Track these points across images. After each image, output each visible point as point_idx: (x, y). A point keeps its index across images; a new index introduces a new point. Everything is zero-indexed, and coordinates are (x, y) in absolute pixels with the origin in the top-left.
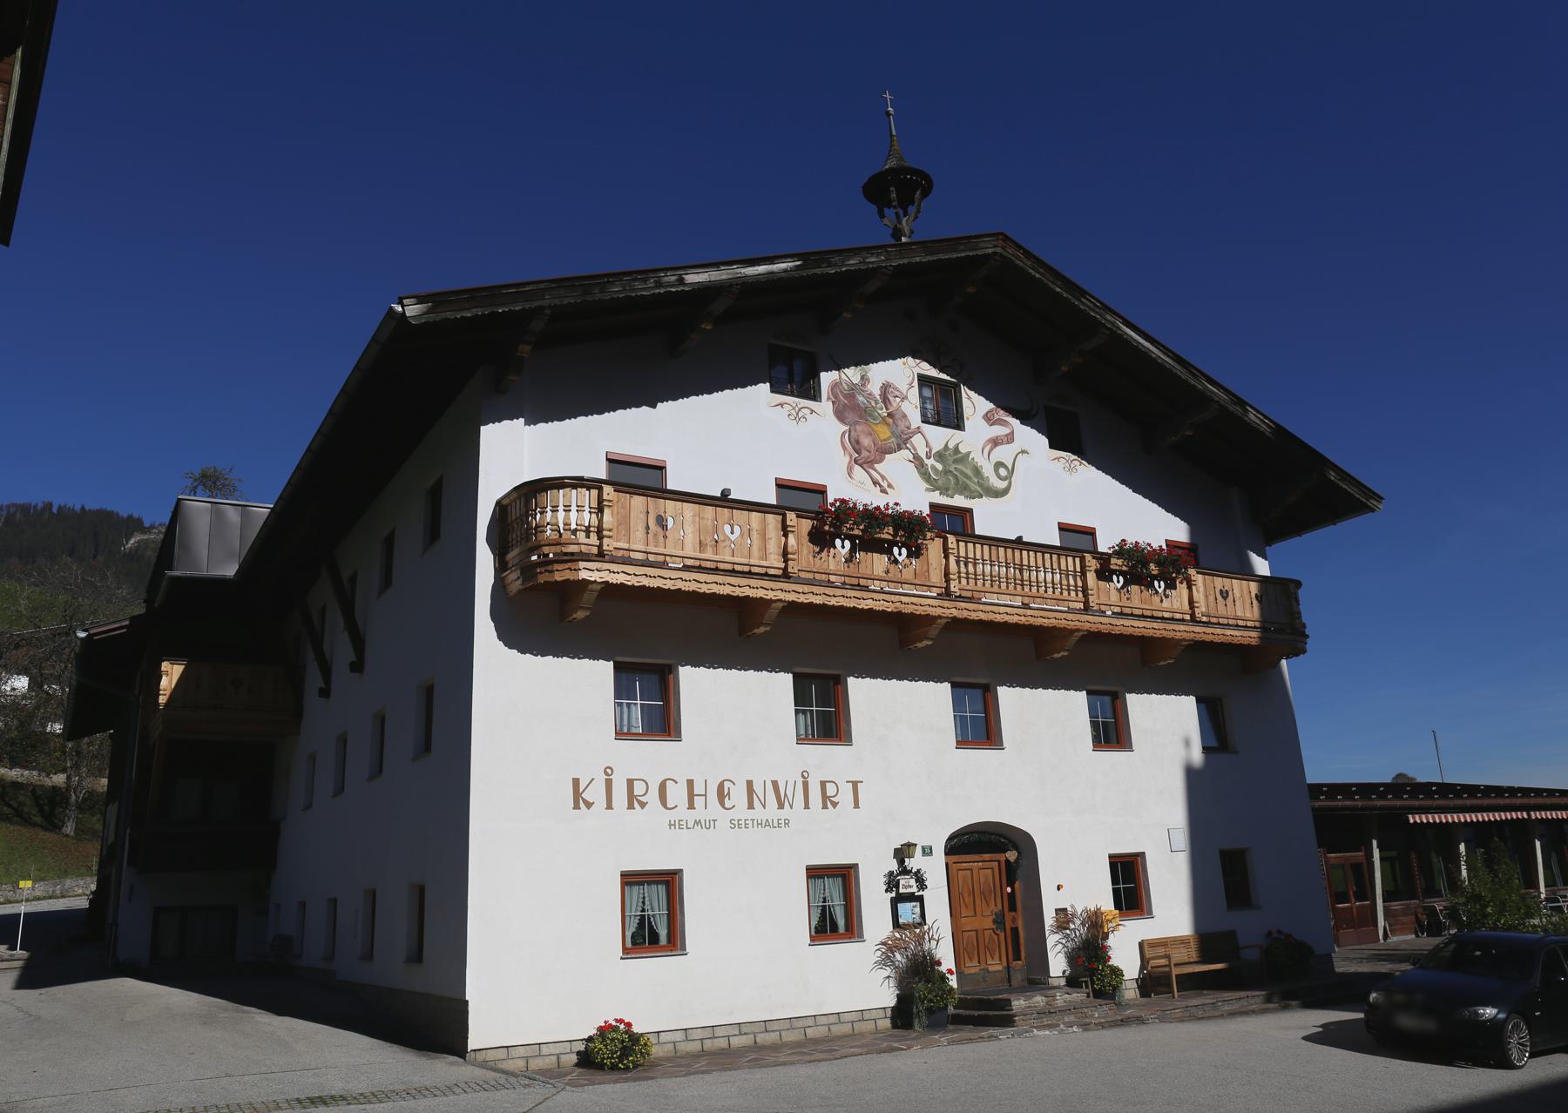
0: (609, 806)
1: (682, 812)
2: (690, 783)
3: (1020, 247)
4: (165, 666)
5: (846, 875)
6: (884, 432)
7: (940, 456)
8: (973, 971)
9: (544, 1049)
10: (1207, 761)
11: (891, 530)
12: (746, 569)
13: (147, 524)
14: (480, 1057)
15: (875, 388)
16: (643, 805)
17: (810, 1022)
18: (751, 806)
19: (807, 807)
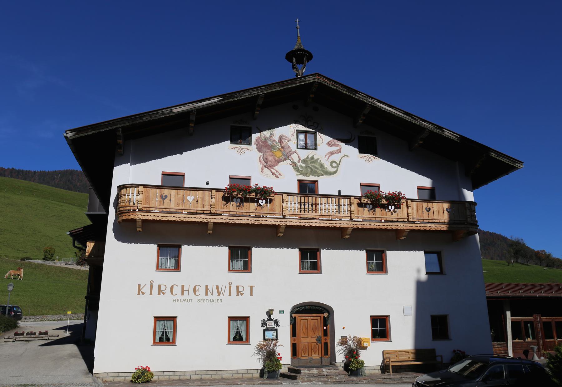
0: (151, 294)
1: (179, 296)
2: (183, 286)
3: (326, 78)
4: (88, 243)
5: (246, 320)
6: (279, 154)
7: (304, 161)
8: (305, 358)
9: (121, 375)
10: (429, 279)
11: (254, 194)
12: (195, 211)
13: (187, 183)
14: (97, 375)
15: (276, 138)
16: (164, 294)
17: (225, 372)
18: (207, 294)
19: (230, 295)
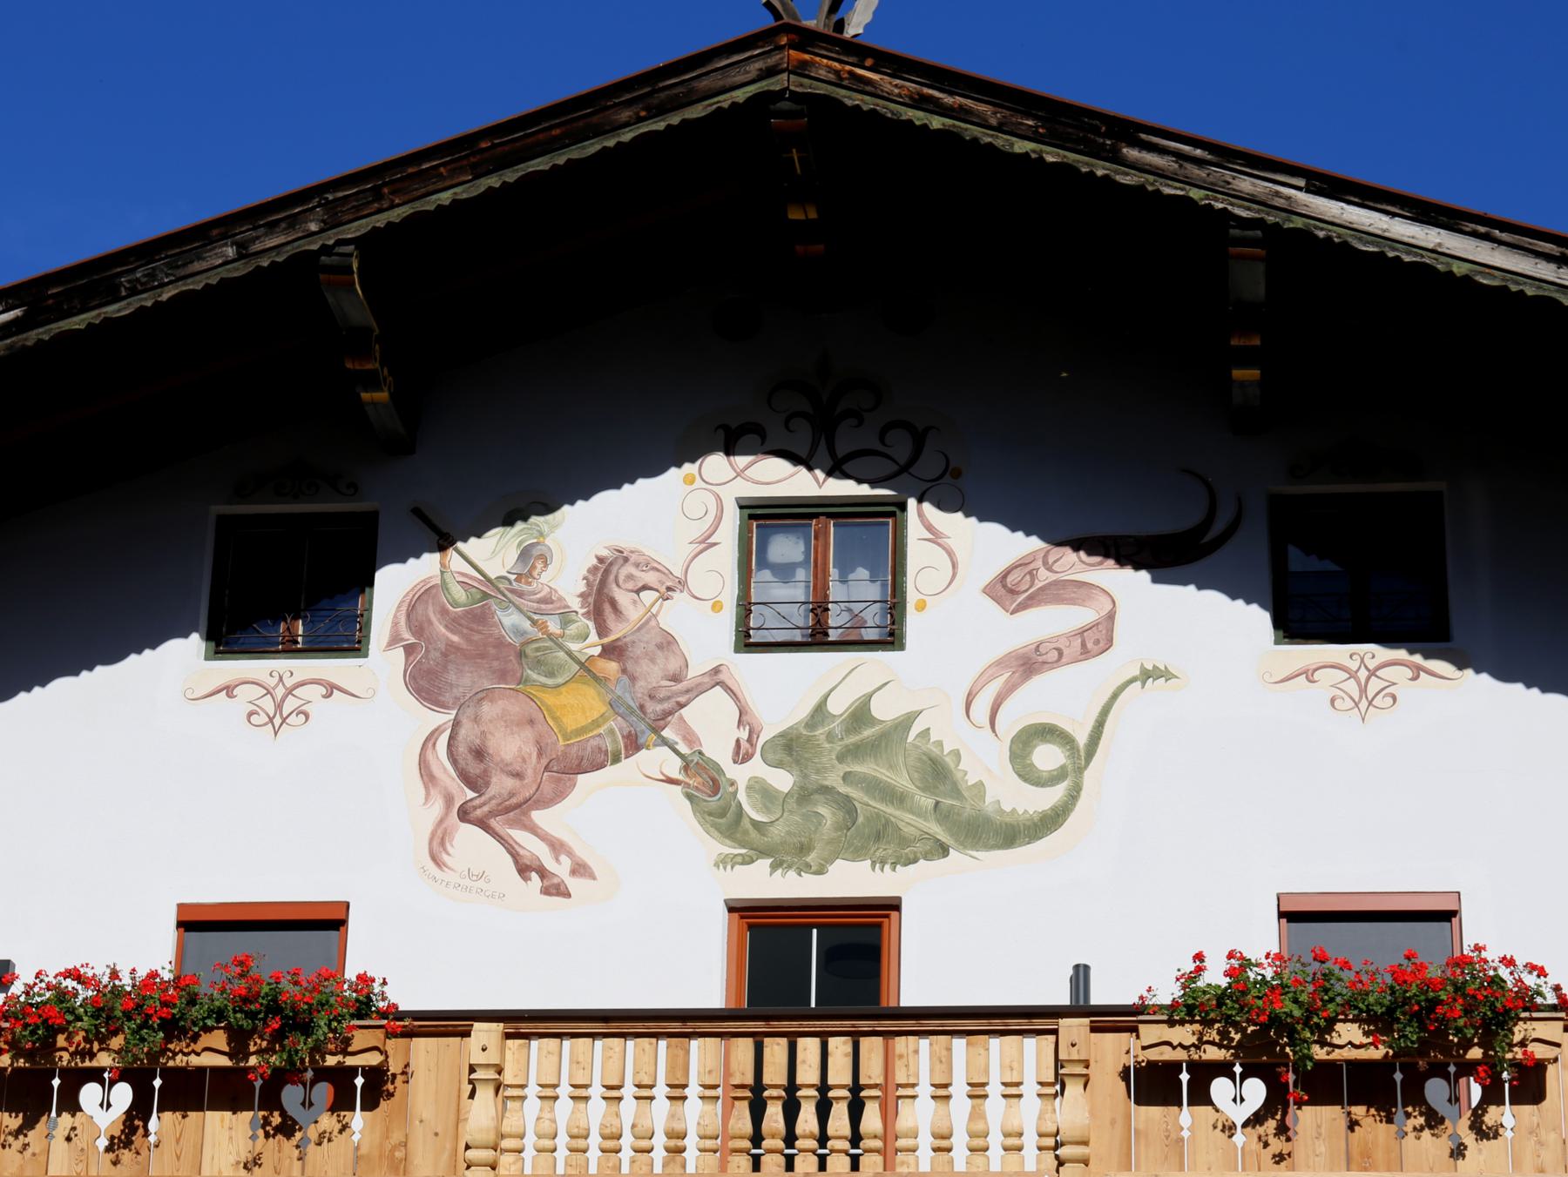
6: (580, 709)
7: (790, 748)
15: (566, 579)
